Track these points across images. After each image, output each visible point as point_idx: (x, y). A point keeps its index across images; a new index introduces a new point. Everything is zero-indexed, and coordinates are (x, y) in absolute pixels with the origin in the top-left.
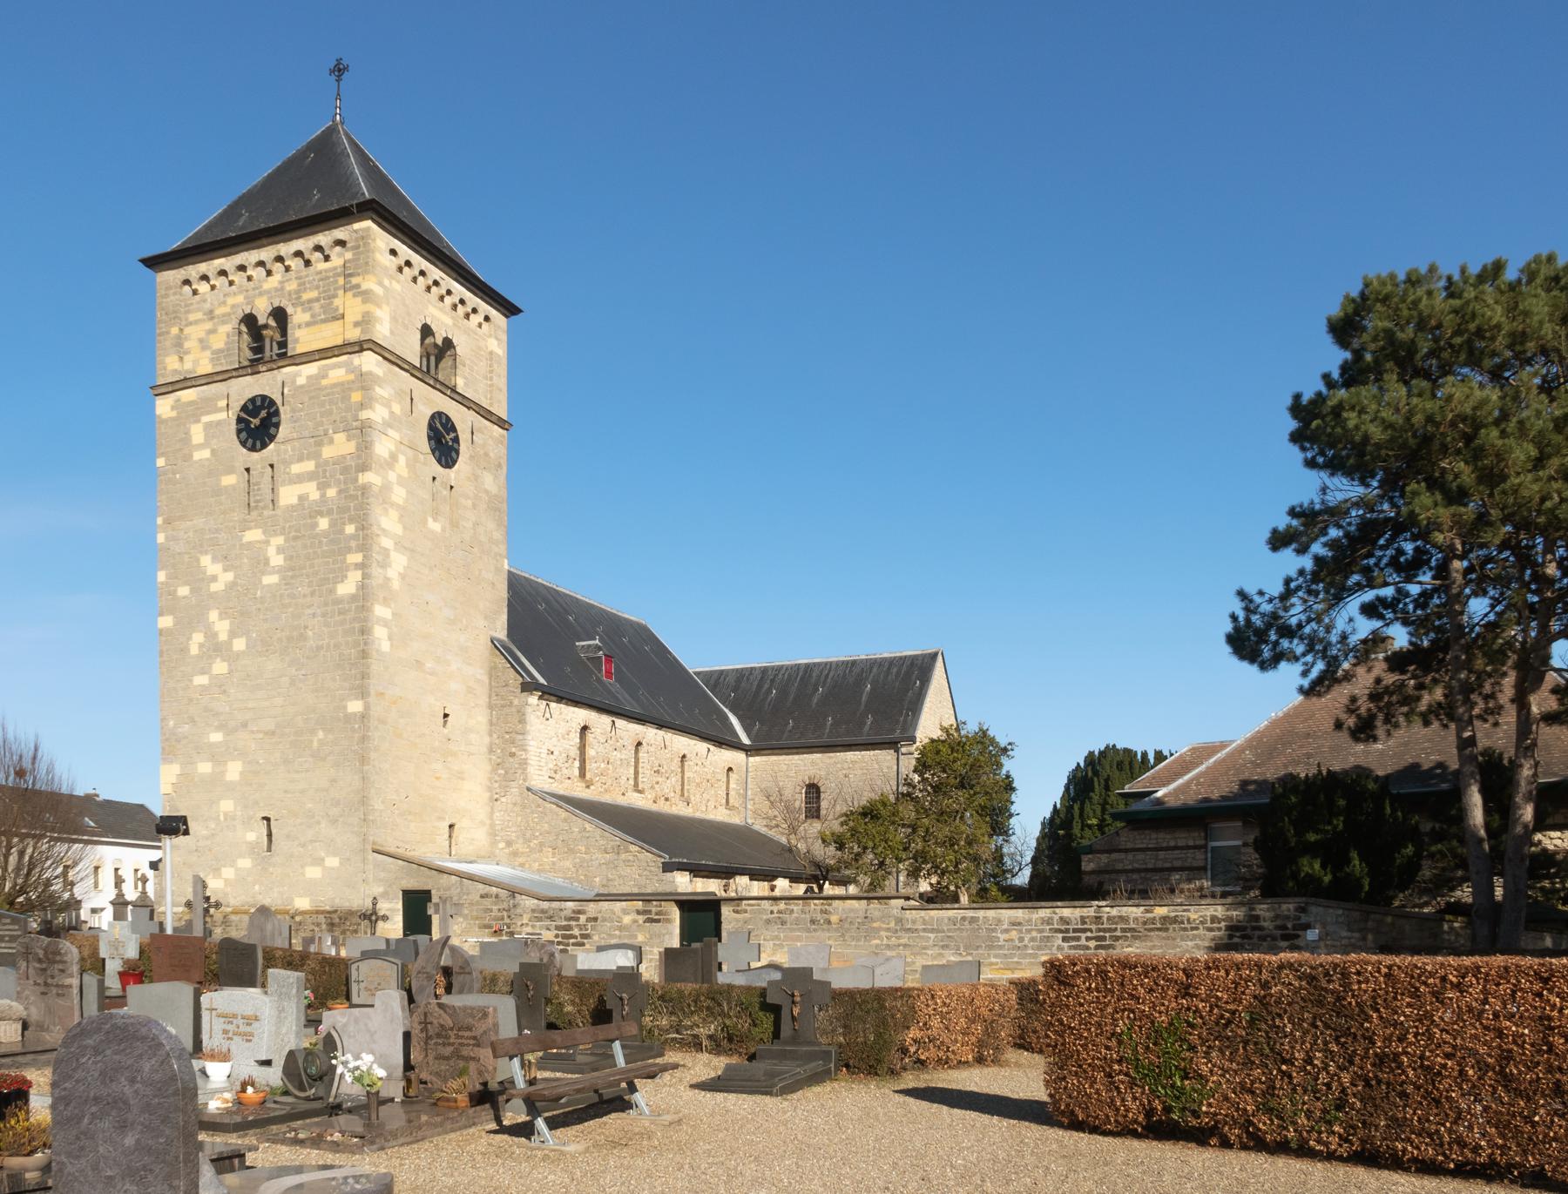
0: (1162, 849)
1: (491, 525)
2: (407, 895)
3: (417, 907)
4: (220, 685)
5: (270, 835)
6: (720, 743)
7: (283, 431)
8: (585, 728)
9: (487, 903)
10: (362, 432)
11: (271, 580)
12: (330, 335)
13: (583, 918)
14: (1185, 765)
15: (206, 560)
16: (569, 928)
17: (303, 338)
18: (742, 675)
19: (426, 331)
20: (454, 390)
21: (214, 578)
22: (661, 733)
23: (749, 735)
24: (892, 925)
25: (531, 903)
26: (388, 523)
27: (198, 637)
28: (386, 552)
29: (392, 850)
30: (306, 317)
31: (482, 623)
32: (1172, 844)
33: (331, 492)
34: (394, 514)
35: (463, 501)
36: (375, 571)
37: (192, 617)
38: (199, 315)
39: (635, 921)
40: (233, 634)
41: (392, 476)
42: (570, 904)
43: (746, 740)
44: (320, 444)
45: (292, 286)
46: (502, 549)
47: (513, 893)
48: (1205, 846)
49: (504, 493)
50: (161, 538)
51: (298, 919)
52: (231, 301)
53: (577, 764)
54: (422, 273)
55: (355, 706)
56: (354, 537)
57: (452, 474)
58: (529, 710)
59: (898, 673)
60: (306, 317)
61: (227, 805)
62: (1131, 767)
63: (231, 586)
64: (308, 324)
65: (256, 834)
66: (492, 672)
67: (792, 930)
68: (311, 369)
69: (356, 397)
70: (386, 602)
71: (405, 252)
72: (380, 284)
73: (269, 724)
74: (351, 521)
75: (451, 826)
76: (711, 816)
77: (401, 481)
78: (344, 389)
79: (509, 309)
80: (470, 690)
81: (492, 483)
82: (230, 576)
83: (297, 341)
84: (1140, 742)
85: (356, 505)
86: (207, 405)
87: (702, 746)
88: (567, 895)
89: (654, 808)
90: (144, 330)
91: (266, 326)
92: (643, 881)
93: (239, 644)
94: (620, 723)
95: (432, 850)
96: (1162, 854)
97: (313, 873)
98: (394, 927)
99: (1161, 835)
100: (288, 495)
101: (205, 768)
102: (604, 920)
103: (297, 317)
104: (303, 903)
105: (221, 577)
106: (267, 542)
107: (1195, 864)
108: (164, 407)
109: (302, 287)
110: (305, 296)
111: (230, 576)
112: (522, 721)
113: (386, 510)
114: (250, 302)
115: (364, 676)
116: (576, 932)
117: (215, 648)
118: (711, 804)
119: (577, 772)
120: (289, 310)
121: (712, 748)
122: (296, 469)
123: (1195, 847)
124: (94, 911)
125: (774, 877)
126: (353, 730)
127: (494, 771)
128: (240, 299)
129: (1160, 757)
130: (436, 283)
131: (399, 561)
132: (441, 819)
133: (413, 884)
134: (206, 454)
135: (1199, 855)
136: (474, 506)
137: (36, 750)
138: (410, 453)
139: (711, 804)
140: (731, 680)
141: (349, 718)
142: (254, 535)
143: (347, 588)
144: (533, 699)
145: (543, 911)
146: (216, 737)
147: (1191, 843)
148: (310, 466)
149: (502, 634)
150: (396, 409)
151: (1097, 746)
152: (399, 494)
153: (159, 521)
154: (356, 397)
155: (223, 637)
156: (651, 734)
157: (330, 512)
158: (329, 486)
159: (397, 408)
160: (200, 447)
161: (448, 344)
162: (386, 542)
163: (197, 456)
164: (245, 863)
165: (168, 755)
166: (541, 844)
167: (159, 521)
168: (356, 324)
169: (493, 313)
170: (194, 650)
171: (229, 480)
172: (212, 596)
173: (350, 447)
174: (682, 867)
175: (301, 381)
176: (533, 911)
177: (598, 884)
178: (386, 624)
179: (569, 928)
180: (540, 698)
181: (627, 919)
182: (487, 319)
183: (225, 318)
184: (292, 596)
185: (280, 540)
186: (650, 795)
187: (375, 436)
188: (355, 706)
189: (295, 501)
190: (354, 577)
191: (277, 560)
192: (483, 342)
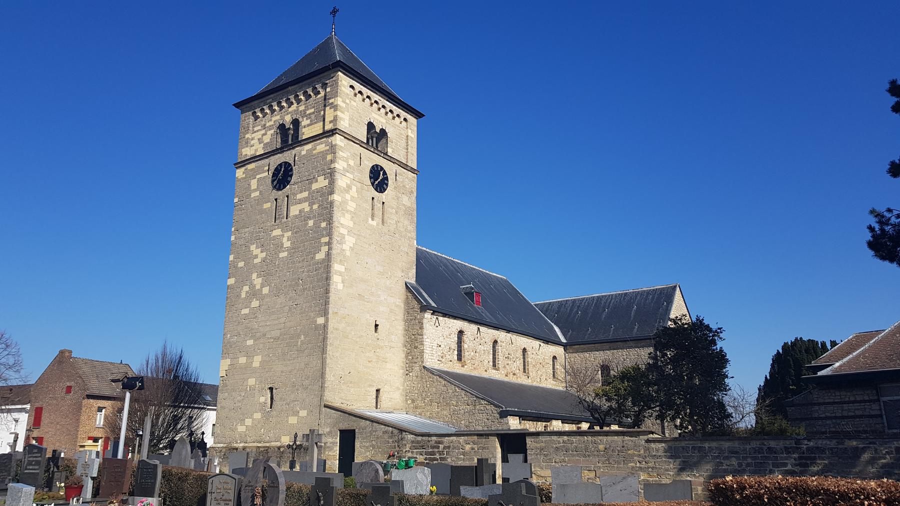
0: (845, 403)
1: (406, 222)
2: (342, 432)
3: (348, 439)
4: (254, 313)
5: (272, 398)
6: (547, 342)
7: (294, 179)
8: (461, 333)
9: (386, 436)
10: (331, 174)
11: (283, 255)
12: (317, 129)
13: (441, 446)
14: (851, 347)
15: (253, 247)
16: (433, 453)
18: (561, 304)
19: (371, 126)
20: (386, 154)
21: (256, 256)
22: (509, 335)
23: (565, 338)
24: (642, 452)
25: (410, 437)
26: (343, 221)
29: (337, 404)
30: (308, 122)
31: (400, 274)
32: (852, 399)
33: (315, 207)
34: (348, 216)
35: (390, 210)
36: (336, 247)
37: (245, 279)
38: (259, 128)
39: (473, 449)
40: (263, 286)
41: (348, 197)
42: (434, 438)
43: (564, 340)
44: (311, 183)
45: (302, 108)
46: (414, 235)
47: (401, 430)
48: (879, 400)
49: (415, 206)
50: (233, 238)
51: (282, 450)
52: (274, 119)
53: (456, 352)
54: (368, 97)
55: (321, 321)
56: (325, 229)
57: (383, 196)
58: (425, 321)
59: (653, 298)
60: (308, 122)
61: (252, 381)
62: (815, 352)
63: (264, 260)
64: (308, 125)
65: (265, 398)
66: (407, 303)
67: (573, 455)
68: (309, 146)
69: (329, 157)
70: (341, 262)
71: (358, 87)
72: (344, 102)
73: (276, 333)
74: (324, 221)
75: (378, 391)
76: (543, 385)
78: (324, 154)
79: (418, 115)
80: (391, 311)
81: (409, 201)
82: (264, 255)
83: (303, 134)
84: (820, 336)
85: (327, 212)
87: (536, 343)
88: (432, 432)
89: (506, 379)
90: (235, 138)
91: (289, 129)
92: (489, 423)
93: (266, 290)
94: (482, 329)
95: (365, 407)
96: (845, 406)
97: (293, 420)
99: (843, 393)
100: (294, 210)
101: (243, 360)
102: (454, 448)
103: (304, 122)
105: (258, 254)
106: (283, 236)
107: (873, 413)
108: (240, 173)
109: (307, 108)
110: (308, 112)
111: (264, 255)
112: (422, 328)
113: (344, 214)
114: (282, 118)
115: (327, 303)
116: (437, 456)
117: (254, 294)
118: (544, 378)
119: (456, 357)
120: (300, 120)
121: (542, 344)
122: (299, 196)
123: (869, 401)
125: (580, 422)
126: (319, 334)
127: (406, 357)
128: (278, 117)
129: (834, 344)
130: (376, 102)
131: (350, 241)
132: (370, 386)
133: (345, 426)
134: (257, 193)
135: (875, 406)
136: (396, 212)
137: (181, 358)
138: (359, 185)
139: (544, 378)
140: (555, 307)
141: (317, 327)
142: (277, 232)
143: (320, 256)
144: (428, 315)
145: (418, 442)
146: (250, 342)
147: (866, 398)
148: (305, 194)
149: (413, 281)
150: (351, 164)
151: (790, 339)
152: (352, 206)
153: (233, 229)
154: (329, 157)
155: (258, 287)
156: (502, 335)
157: (314, 217)
158: (314, 203)
159: (352, 163)
160: (255, 190)
161: (383, 133)
162: (343, 231)
163: (253, 195)
164: (258, 416)
165: (225, 354)
166: (431, 401)
167: (233, 229)
168: (331, 122)
169: (409, 117)
170: (243, 295)
172: (255, 266)
173: (326, 182)
174: (514, 414)
175: (304, 153)
176: (413, 442)
177: (463, 426)
178: (341, 274)
179: (433, 453)
180: (432, 314)
181: (468, 447)
182: (405, 120)
183: (270, 128)
184: (293, 263)
185: (290, 233)
186: (503, 372)
187: (337, 176)
188: (321, 321)
189: (297, 213)
191: (287, 244)
192: (403, 133)
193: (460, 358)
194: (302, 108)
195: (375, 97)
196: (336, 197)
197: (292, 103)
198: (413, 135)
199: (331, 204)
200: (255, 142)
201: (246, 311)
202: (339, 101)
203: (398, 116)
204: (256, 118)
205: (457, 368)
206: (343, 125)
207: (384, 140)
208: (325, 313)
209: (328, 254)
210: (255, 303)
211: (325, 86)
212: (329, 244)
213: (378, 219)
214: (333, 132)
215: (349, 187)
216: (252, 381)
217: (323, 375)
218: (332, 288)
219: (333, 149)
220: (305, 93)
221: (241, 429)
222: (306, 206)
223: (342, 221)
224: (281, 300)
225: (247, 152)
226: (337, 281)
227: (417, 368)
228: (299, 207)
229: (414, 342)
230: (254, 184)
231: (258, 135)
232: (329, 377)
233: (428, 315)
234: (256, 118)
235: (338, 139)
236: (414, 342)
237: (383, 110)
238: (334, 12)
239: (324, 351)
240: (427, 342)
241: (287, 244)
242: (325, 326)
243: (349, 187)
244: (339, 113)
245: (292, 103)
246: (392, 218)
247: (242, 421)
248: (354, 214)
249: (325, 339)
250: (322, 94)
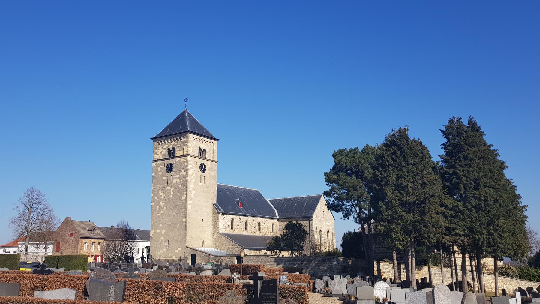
3: (194, 257)
4: (161, 215)
7: (174, 170)
10: (187, 170)
11: (171, 196)
15: (160, 192)
17: (178, 153)
26: (191, 186)
27: (158, 207)
28: (191, 191)
29: (190, 247)
33: (182, 181)
34: (193, 184)
36: (189, 195)
40: (164, 206)
45: (176, 144)
55: (184, 220)
61: (162, 238)
63: (164, 197)
65: (167, 244)
68: (179, 159)
69: (186, 164)
71: (195, 136)
73: (170, 223)
77: (194, 178)
78: (184, 163)
85: (185, 183)
86: (161, 165)
93: (165, 208)
97: (176, 251)
98: (189, 262)
101: (158, 231)
103: (177, 149)
104: (174, 258)
115: (186, 214)
117: (161, 209)
122: (176, 176)
124: (137, 259)
131: (193, 192)
141: (183, 222)
142: (168, 188)
143: (184, 198)
146: (161, 225)
148: (178, 176)
150: (193, 164)
152: (194, 180)
154: (186, 164)
159: (193, 165)
162: (191, 189)
164: (164, 250)
170: (157, 209)
171: (165, 178)
173: (185, 173)
178: (190, 204)
183: (165, 149)
188: (184, 220)
190: (185, 196)
191: (172, 193)
194: (176, 144)
195: (201, 138)
196: (189, 178)
198: (215, 148)
199: (187, 180)
200: (159, 153)
201: (158, 215)
202: (189, 144)
204: (159, 144)
206: (190, 152)
207: (204, 152)
208: (186, 218)
209: (186, 198)
210: (162, 212)
211: (184, 137)
212: (186, 194)
213: (203, 182)
214: (187, 155)
215: (193, 174)
216: (162, 238)
217: (186, 237)
218: (188, 209)
219: (187, 161)
220: (177, 139)
221: (159, 254)
222: (178, 180)
223: (191, 186)
224: (171, 212)
225: (156, 157)
226: (189, 206)
227: (216, 233)
228: (176, 180)
229: (215, 224)
230: (159, 169)
231: (161, 151)
232: (188, 238)
233: (220, 215)
234: (159, 144)
235: (189, 158)
236: (215, 224)
238: (186, 100)
239: (186, 230)
240: (220, 224)
241: (172, 193)
242: (186, 222)
243: (193, 174)
244: (189, 149)
246: (208, 181)
247: (159, 252)
248: (194, 183)
249: (186, 226)
250: (183, 140)
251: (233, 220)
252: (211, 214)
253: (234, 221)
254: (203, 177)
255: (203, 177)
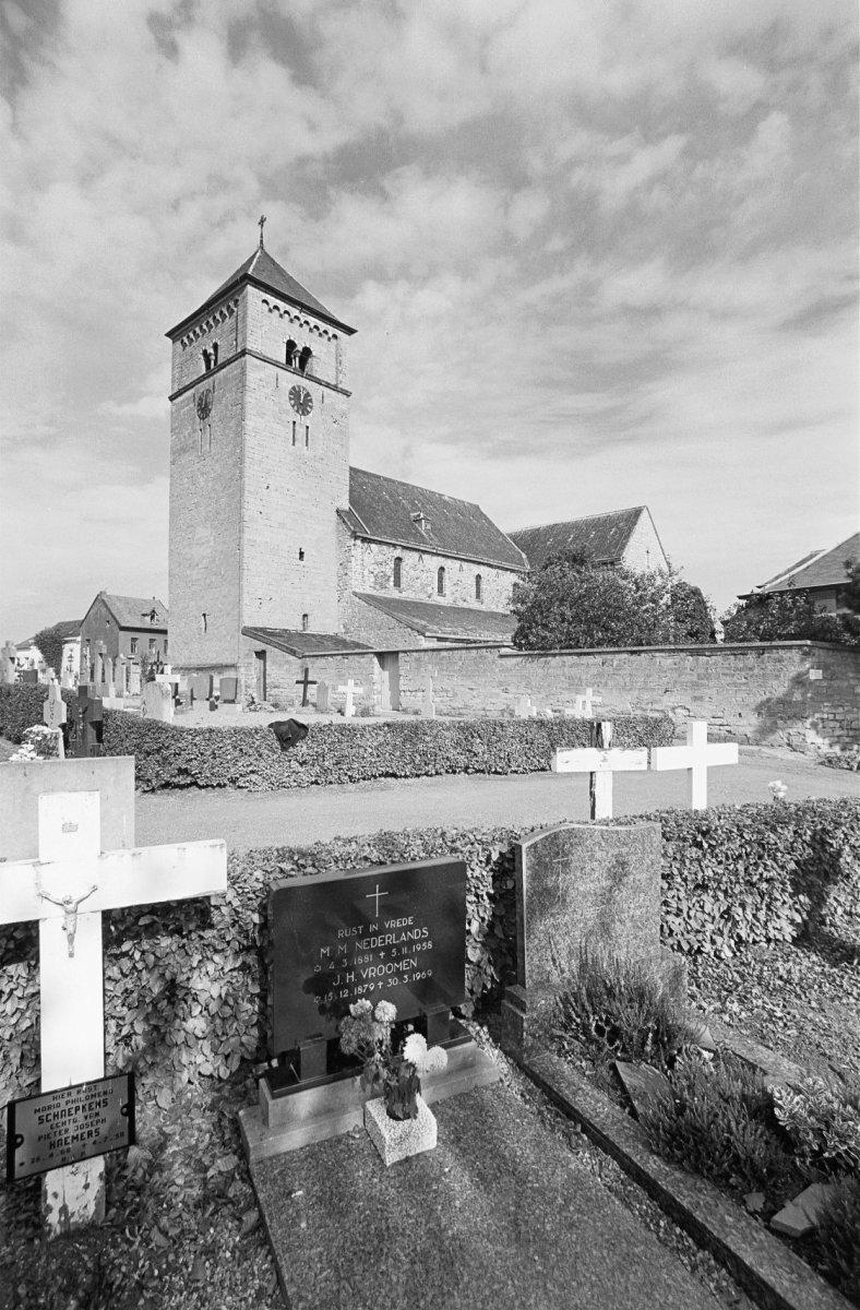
19: (291, 345)
54: (286, 312)
71: (273, 301)
130: (297, 317)
161: (307, 352)
193: (397, 583)
197: (212, 327)
203: (326, 332)
205: (394, 594)
214: (244, 353)
237: (316, 332)
245: (212, 327)
251: (399, 559)
252: (333, 538)
253: (403, 564)
254: (301, 431)
255: (301, 431)
